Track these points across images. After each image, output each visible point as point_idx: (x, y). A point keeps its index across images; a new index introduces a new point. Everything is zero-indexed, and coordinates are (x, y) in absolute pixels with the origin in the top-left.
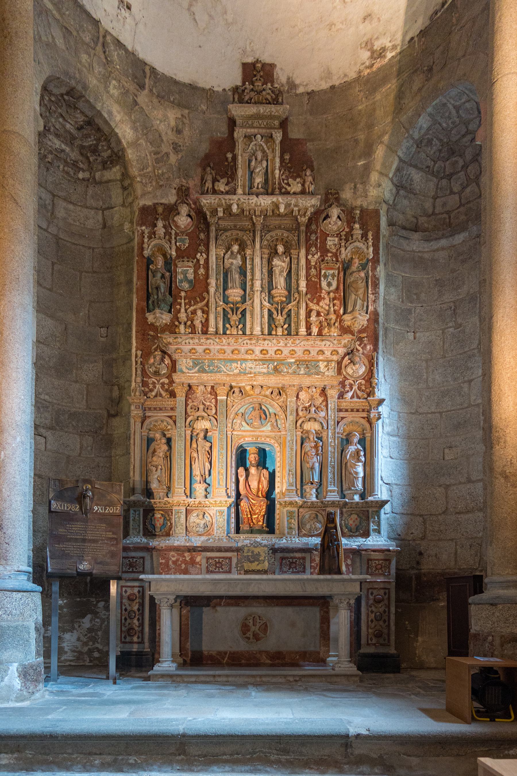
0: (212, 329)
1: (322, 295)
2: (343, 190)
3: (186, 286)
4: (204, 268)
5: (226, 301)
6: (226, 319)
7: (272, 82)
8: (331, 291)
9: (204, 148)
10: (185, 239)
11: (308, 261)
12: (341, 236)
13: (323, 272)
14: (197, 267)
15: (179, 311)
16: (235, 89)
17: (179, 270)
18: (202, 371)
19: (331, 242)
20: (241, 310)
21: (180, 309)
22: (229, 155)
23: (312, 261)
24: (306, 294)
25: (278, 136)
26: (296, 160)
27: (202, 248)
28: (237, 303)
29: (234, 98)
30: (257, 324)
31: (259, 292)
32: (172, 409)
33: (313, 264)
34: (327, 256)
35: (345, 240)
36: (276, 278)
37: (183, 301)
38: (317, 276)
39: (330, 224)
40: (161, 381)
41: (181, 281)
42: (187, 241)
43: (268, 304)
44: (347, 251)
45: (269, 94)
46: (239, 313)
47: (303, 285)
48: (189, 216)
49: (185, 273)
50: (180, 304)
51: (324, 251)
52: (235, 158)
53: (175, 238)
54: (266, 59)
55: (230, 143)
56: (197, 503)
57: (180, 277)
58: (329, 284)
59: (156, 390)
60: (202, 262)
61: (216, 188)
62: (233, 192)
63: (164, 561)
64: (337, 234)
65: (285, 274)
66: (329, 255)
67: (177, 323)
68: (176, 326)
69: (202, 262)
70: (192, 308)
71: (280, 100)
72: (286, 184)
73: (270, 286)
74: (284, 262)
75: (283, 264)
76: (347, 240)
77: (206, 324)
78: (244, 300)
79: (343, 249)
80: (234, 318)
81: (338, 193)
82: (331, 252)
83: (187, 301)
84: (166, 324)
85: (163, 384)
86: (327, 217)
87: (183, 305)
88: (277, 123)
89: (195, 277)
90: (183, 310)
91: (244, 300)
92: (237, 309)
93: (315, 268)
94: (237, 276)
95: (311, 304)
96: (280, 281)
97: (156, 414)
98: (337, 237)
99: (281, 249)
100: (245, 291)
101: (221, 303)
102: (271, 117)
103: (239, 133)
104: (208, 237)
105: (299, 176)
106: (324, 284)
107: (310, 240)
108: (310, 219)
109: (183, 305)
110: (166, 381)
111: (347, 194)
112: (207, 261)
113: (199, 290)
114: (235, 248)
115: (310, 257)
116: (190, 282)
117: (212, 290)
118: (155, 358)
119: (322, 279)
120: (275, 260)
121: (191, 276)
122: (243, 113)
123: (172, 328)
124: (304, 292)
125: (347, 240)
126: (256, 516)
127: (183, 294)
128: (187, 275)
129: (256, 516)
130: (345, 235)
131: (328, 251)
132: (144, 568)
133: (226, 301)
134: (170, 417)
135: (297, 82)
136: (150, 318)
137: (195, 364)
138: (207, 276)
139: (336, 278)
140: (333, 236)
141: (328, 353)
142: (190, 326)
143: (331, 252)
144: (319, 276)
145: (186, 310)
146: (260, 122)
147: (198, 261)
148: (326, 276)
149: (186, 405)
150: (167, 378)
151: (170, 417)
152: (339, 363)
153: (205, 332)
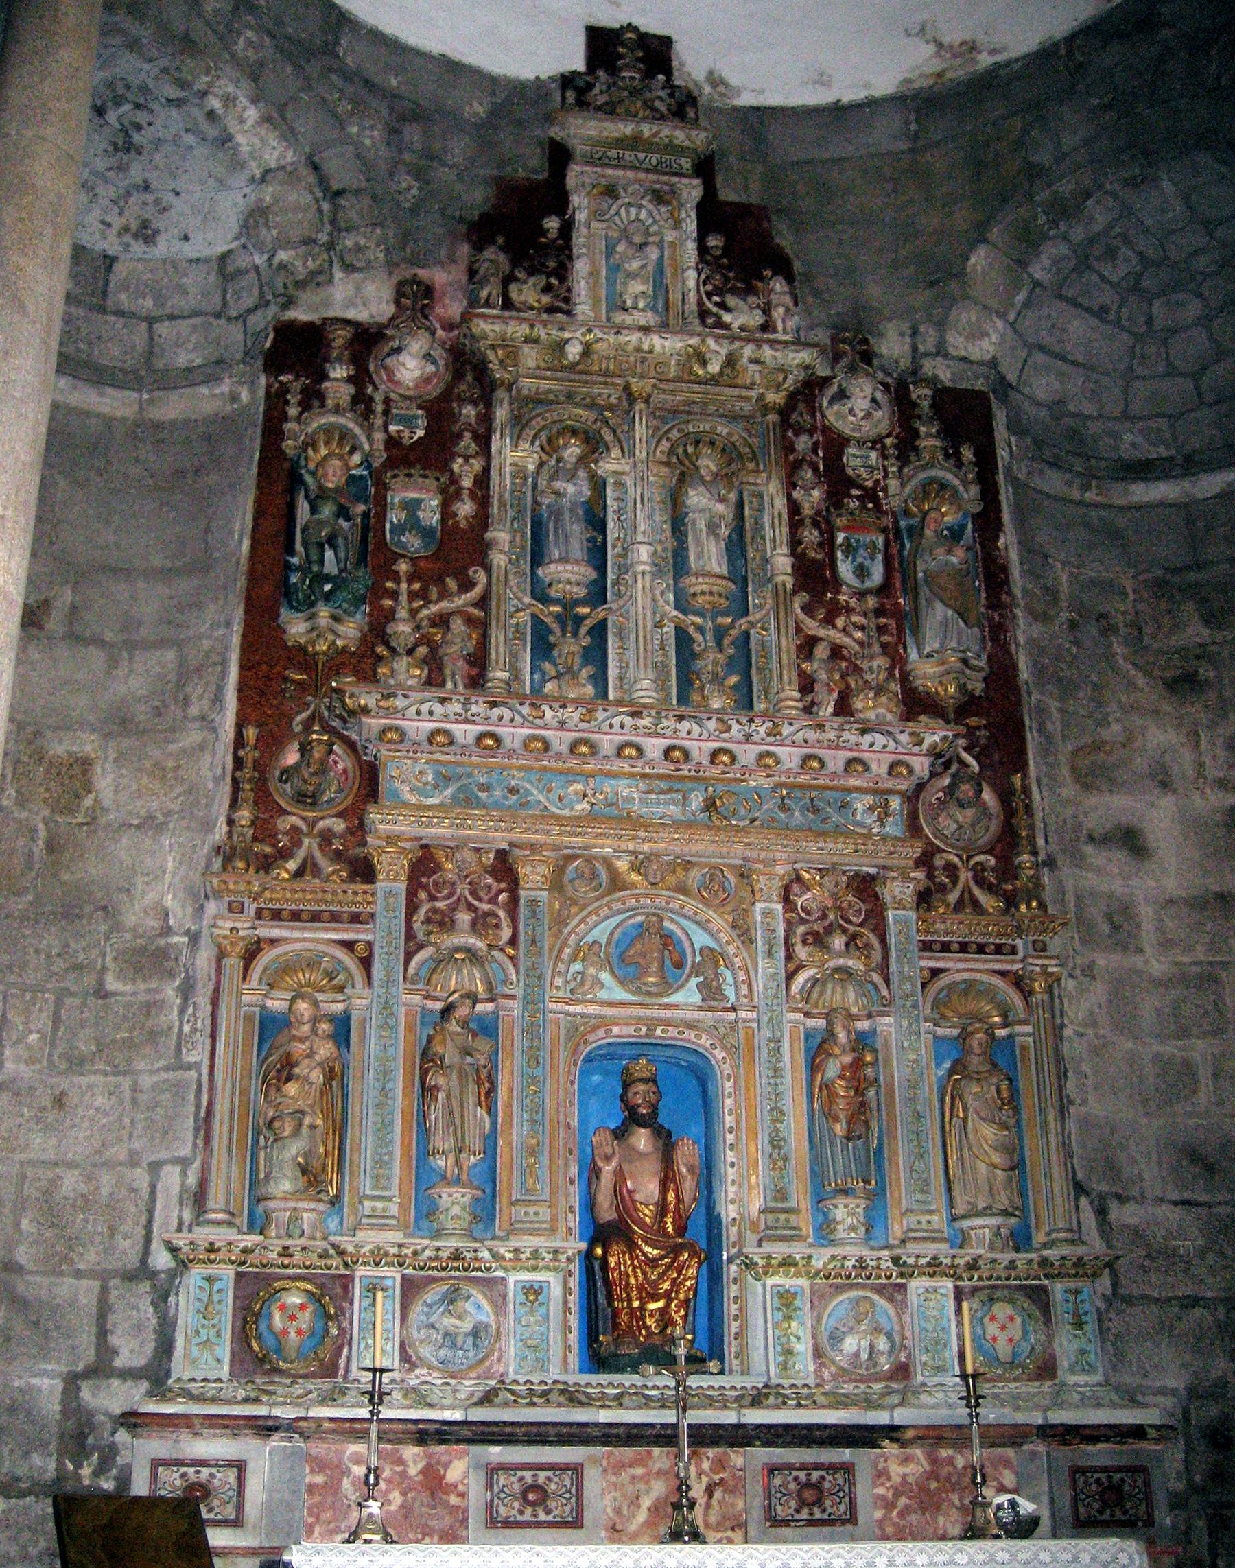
0: (499, 674)
1: (842, 598)
2: (881, 335)
3: (413, 542)
4: (472, 495)
5: (540, 593)
6: (543, 647)
7: (668, 73)
8: (868, 592)
9: (478, 198)
10: (416, 417)
11: (794, 508)
12: (884, 447)
13: (840, 537)
14: (449, 495)
15: (390, 616)
16: (567, 80)
17: (395, 498)
18: (466, 800)
19: (856, 460)
20: (589, 623)
21: (393, 611)
22: (552, 224)
23: (806, 505)
24: (795, 592)
25: (692, 191)
26: (742, 248)
27: (467, 443)
28: (577, 603)
29: (564, 98)
30: (637, 668)
31: (648, 578)
32: (355, 918)
33: (807, 511)
34: (850, 496)
35: (898, 458)
36: (698, 542)
37: (404, 586)
38: (820, 545)
39: (851, 411)
40: (321, 824)
41: (399, 529)
42: (422, 422)
43: (675, 613)
44: (908, 489)
45: (660, 98)
46: (583, 630)
47: (782, 562)
48: (428, 357)
49: (412, 507)
50: (394, 595)
51: (838, 483)
52: (567, 229)
53: (386, 413)
54: (650, 24)
55: (554, 196)
56: (445, 1254)
57: (395, 516)
58: (862, 572)
59: (301, 854)
60: (467, 483)
61: (514, 295)
62: (560, 305)
63: (319, 1479)
64: (874, 442)
65: (724, 532)
66: (855, 492)
67: (380, 650)
68: (379, 658)
69: (467, 483)
70: (434, 608)
71: (691, 113)
72: (716, 304)
73: (677, 563)
74: (722, 500)
75: (720, 508)
76: (903, 459)
77: (479, 662)
78: (598, 594)
79: (893, 484)
80: (570, 647)
81: (865, 341)
82: (859, 487)
83: (417, 586)
84: (344, 650)
85: (326, 838)
86: (842, 395)
87: (403, 599)
88: (686, 163)
89: (443, 521)
90: (402, 613)
91: (598, 594)
92: (579, 620)
93: (815, 524)
94: (577, 531)
95: (812, 626)
96: (709, 556)
97: (296, 934)
98: (872, 448)
99: (708, 463)
100: (601, 568)
101: (527, 600)
102: (671, 148)
103: (575, 175)
104: (486, 419)
105: (750, 290)
106: (845, 569)
107: (793, 450)
108: (792, 397)
109: (403, 599)
110: (339, 826)
111: (892, 346)
112: (483, 480)
113: (458, 551)
114: (573, 451)
115: (796, 494)
116: (426, 533)
117: (499, 559)
118: (304, 750)
119: (839, 554)
120: (691, 493)
121: (430, 515)
122: (592, 133)
123: (366, 661)
124: (789, 586)
125: (903, 459)
126: (660, 1304)
127: (403, 567)
128: (420, 514)
129: (660, 1304)
130: (896, 447)
131: (852, 483)
132: (240, 1507)
133: (540, 593)
134: (349, 945)
135: (734, 81)
136: (296, 628)
137: (444, 779)
138: (482, 519)
139: (880, 557)
140: (861, 443)
141: (879, 767)
142: (425, 660)
143: (859, 487)
144: (828, 544)
145: (413, 612)
146: (641, 156)
147: (454, 480)
148: (849, 549)
149: (412, 908)
150: (340, 815)
151: (349, 945)
152: (913, 798)
153: (477, 681)
